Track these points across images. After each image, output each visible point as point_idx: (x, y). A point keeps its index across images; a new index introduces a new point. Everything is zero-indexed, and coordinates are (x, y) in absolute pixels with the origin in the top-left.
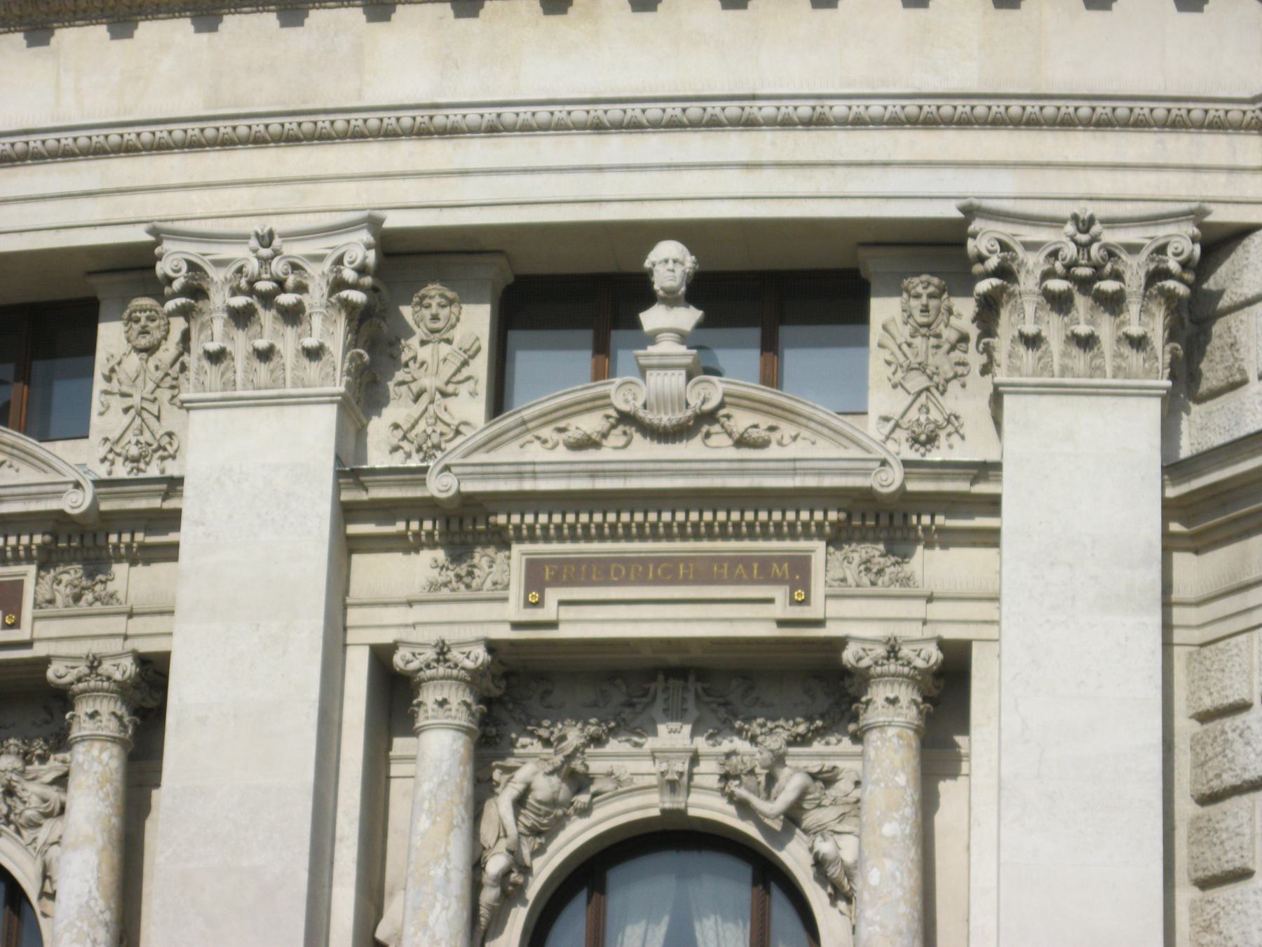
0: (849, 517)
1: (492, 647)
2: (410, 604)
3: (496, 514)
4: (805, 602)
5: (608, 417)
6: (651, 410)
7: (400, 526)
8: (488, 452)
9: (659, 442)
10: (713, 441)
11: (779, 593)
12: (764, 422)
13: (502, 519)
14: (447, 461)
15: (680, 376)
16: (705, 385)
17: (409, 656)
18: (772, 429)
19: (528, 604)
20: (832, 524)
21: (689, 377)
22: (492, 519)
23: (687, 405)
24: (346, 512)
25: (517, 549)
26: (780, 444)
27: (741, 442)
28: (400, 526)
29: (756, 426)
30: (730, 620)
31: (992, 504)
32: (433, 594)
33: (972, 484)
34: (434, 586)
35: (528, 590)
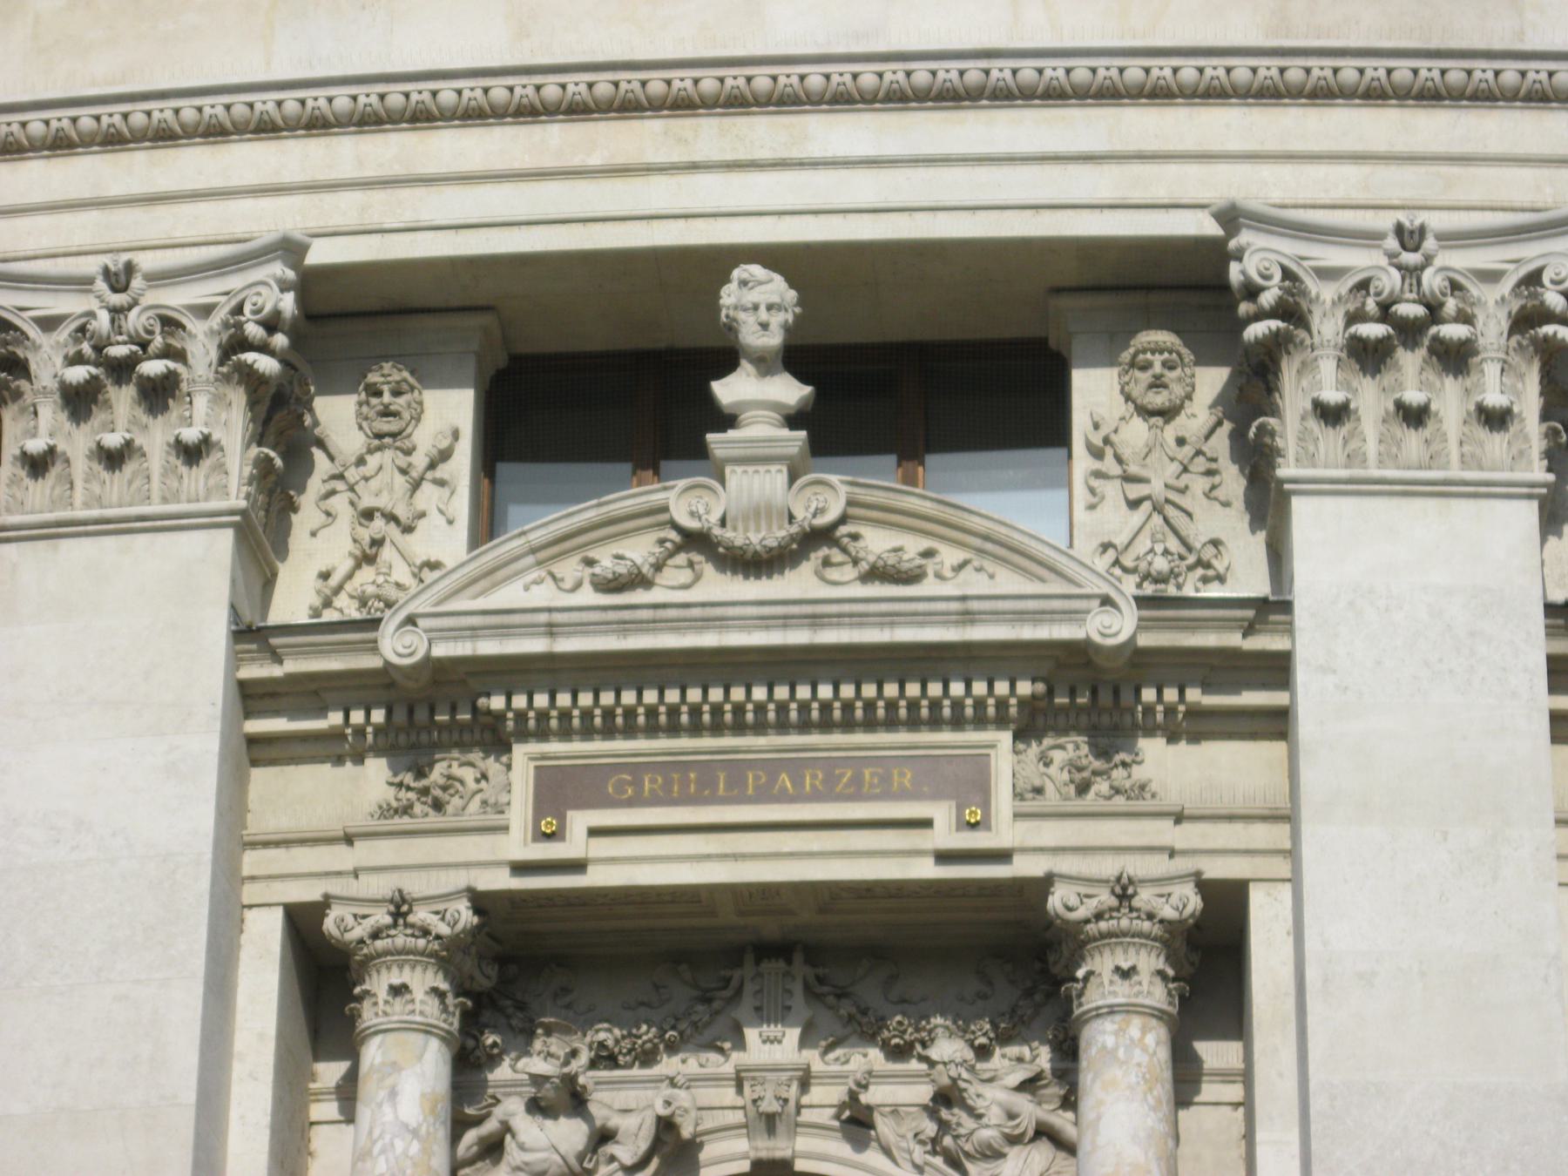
0: (1050, 692)
1: (481, 902)
2: (349, 839)
5: (662, 542)
6: (735, 529)
7: (335, 718)
8: (475, 597)
9: (746, 577)
11: (941, 813)
12: (913, 545)
13: (497, 703)
14: (411, 608)
15: (776, 477)
16: (818, 489)
17: (350, 921)
20: (1022, 702)
21: (793, 477)
22: (482, 702)
23: (791, 518)
24: (252, 697)
25: (521, 753)
27: (877, 574)
28: (335, 718)
30: (736, 857)
31: (1278, 669)
33: (1245, 636)
34: (387, 811)
35: (539, 814)
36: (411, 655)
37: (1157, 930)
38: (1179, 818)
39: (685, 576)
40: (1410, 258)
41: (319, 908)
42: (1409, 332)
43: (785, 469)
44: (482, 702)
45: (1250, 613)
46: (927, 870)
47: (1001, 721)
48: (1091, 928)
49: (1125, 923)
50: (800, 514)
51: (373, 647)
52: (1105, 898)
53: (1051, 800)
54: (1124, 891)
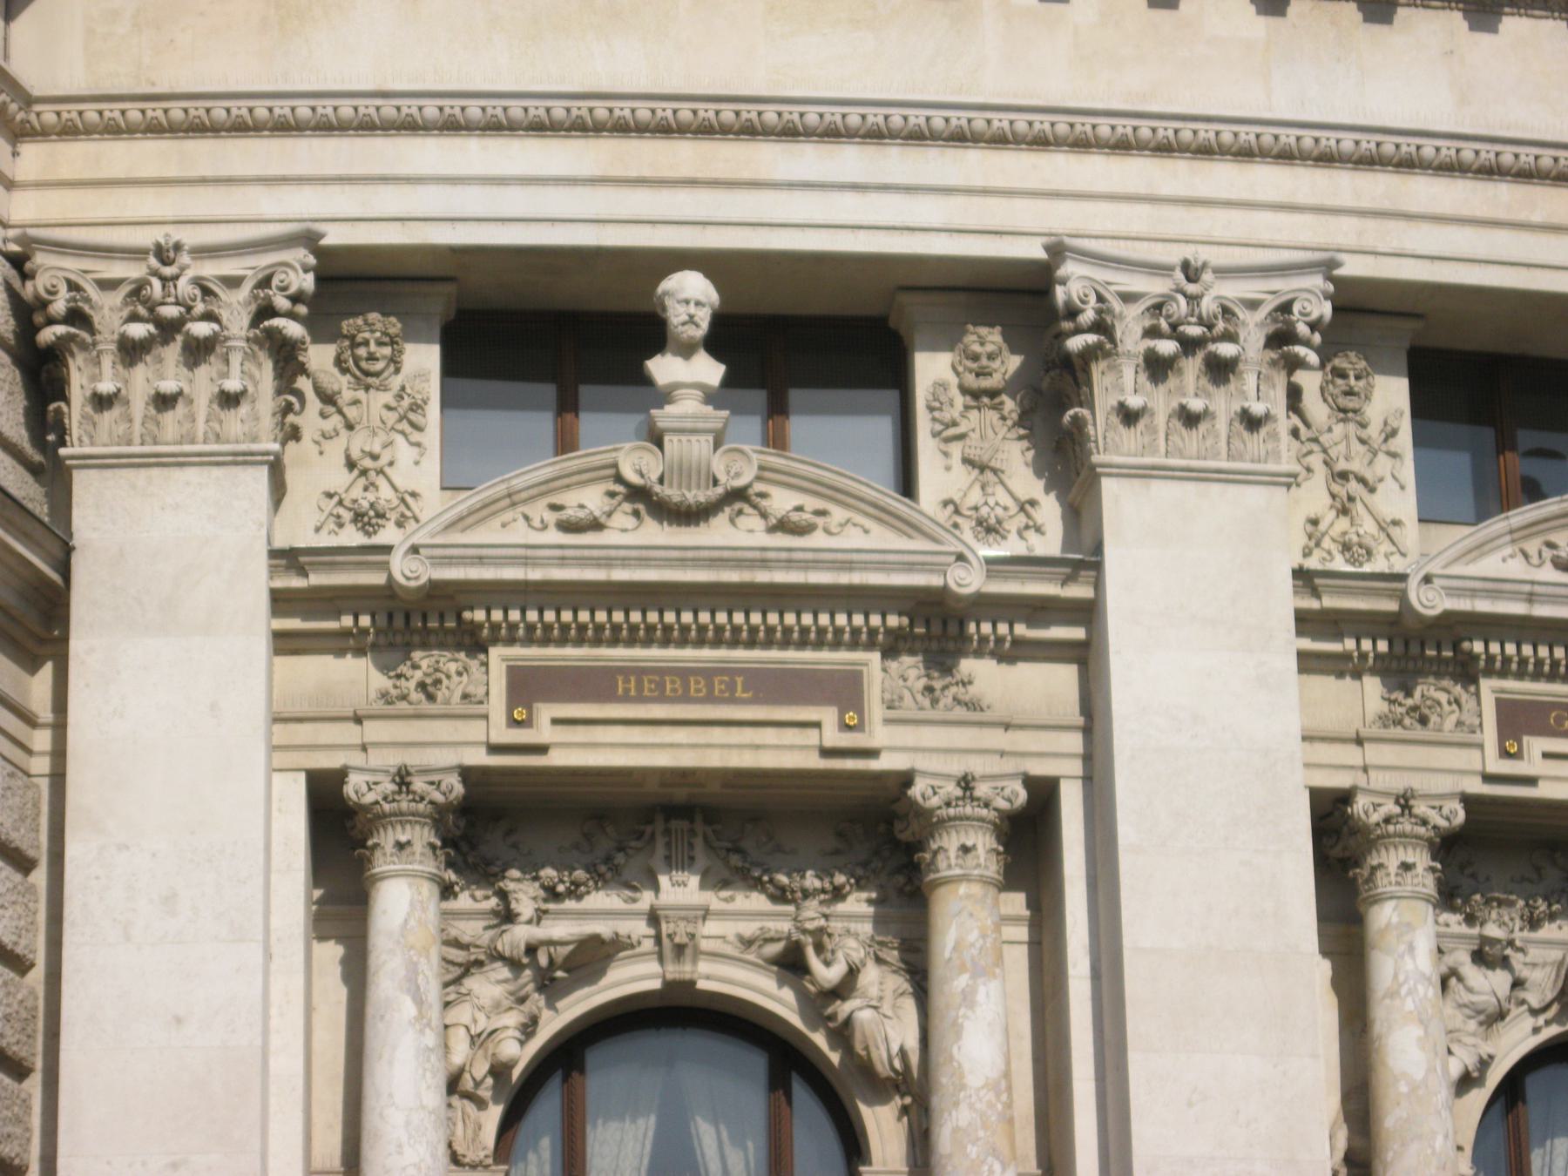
1: (467, 774)
3: (472, 609)
4: (858, 728)
5: (612, 494)
6: (671, 485)
7: (347, 621)
8: (463, 530)
9: (679, 525)
10: (743, 521)
11: (828, 715)
13: (479, 615)
15: (706, 442)
16: (736, 456)
17: (364, 788)
18: (821, 513)
19: (514, 723)
20: (889, 632)
22: (467, 615)
23: (716, 482)
24: (281, 602)
25: (496, 653)
26: (828, 532)
27: (782, 526)
28: (347, 621)
29: (799, 509)
31: (1089, 613)
32: (390, 706)
36: (417, 578)
37: (992, 815)
38: (1007, 727)
39: (630, 522)
40: (1192, 288)
41: (341, 775)
42: (1189, 346)
43: (711, 439)
44: (467, 615)
45: (1068, 570)
46: (814, 762)
47: (871, 645)
48: (943, 812)
49: (968, 810)
50: (722, 478)
51: (385, 566)
52: (952, 789)
53: (908, 709)
54: (966, 783)
